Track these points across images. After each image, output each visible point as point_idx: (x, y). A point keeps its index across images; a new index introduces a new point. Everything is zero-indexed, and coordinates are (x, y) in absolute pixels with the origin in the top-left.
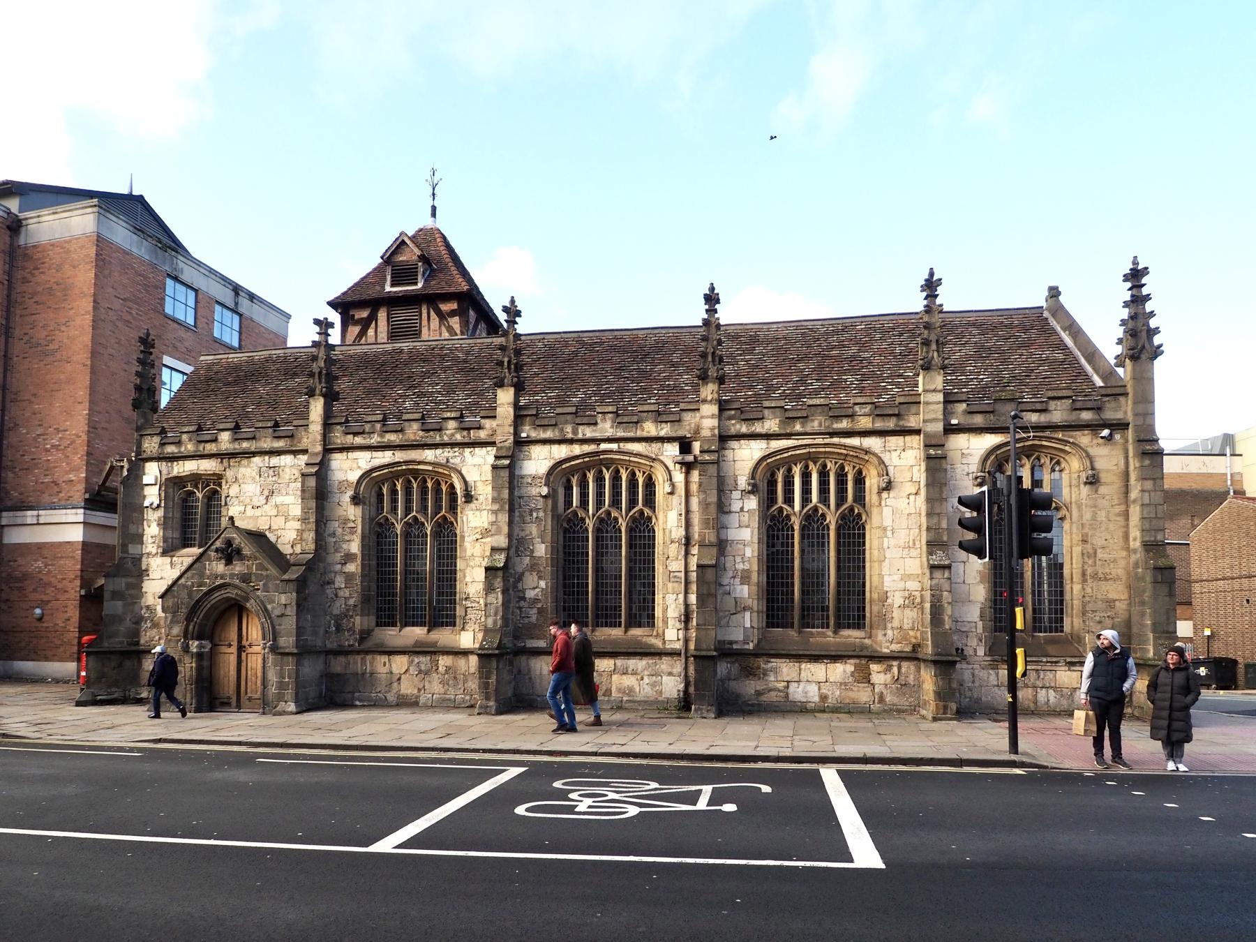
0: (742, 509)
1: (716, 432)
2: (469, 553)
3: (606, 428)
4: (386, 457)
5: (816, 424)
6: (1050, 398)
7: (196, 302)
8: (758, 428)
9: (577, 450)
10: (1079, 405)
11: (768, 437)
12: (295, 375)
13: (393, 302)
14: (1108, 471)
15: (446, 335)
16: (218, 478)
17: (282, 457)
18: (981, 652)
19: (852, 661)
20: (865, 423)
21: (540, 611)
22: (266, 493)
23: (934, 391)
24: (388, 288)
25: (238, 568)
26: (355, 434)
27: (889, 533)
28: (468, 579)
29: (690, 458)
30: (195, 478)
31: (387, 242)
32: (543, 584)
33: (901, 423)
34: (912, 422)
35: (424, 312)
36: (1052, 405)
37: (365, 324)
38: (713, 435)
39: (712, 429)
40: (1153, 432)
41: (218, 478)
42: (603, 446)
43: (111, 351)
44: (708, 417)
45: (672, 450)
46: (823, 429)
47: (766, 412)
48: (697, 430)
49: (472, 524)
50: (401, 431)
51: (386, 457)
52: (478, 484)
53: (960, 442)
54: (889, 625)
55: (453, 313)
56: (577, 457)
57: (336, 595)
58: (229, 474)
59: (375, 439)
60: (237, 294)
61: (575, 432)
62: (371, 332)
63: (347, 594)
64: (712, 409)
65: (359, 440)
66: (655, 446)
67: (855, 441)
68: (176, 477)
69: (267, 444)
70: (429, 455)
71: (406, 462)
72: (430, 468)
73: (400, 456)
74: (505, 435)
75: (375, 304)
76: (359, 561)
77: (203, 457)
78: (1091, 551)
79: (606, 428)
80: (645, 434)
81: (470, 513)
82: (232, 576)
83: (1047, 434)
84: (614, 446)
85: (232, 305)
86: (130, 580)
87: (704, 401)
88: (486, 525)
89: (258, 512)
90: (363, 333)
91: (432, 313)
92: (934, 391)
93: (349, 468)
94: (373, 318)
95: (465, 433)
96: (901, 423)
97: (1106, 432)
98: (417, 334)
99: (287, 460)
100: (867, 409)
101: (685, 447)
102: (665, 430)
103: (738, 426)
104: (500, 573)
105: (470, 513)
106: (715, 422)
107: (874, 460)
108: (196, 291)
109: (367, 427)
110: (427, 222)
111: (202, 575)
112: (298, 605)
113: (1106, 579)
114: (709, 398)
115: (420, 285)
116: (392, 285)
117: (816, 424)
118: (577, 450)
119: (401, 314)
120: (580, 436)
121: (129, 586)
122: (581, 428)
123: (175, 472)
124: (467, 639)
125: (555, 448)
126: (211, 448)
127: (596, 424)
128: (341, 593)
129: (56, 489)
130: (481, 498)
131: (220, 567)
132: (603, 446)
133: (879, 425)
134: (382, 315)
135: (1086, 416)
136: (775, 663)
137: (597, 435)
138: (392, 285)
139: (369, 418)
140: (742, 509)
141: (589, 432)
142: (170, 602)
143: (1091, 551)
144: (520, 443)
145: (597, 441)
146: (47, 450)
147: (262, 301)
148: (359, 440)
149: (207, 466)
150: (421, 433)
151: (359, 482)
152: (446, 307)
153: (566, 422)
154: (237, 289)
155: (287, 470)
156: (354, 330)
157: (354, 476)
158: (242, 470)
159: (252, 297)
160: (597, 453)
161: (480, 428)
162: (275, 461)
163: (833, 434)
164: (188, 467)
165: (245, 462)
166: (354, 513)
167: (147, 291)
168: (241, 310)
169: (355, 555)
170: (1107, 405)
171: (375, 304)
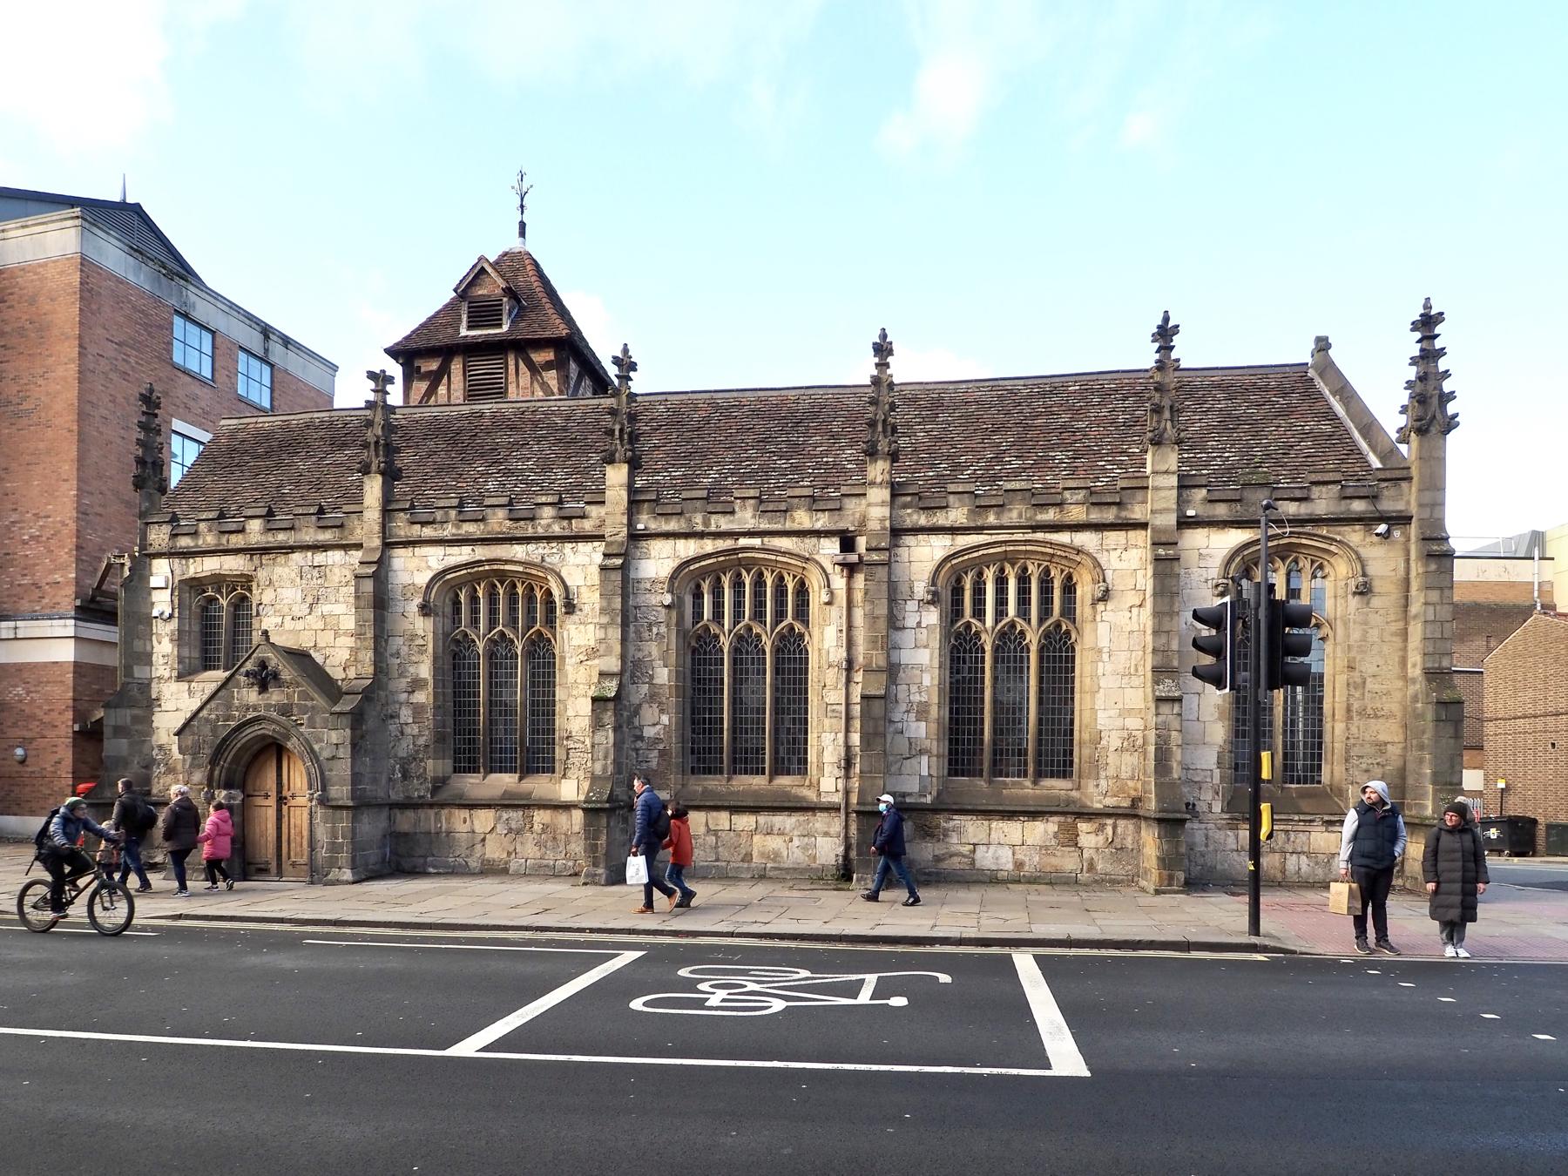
0: (919, 624)
1: (887, 524)
2: (571, 679)
3: (746, 518)
4: (463, 554)
5: (1014, 514)
6: (1313, 483)
7: (214, 347)
8: (941, 519)
9: (709, 546)
10: (1349, 492)
11: (953, 530)
12: (344, 445)
13: (472, 350)
14: (1382, 578)
15: (540, 394)
16: (247, 580)
17: (330, 553)
18: (1217, 807)
19: (1056, 819)
20: (1077, 514)
21: (663, 753)
22: (310, 600)
23: (1166, 472)
24: (464, 332)
25: (275, 696)
26: (424, 524)
27: (1105, 657)
28: (570, 713)
29: (853, 558)
30: (218, 580)
31: (460, 269)
32: (665, 719)
33: (1123, 514)
34: (1137, 513)
35: (511, 363)
36: (1316, 491)
37: (435, 379)
38: (884, 528)
39: (882, 520)
40: (1443, 528)
41: (247, 580)
42: (743, 542)
43: (105, 412)
44: (876, 505)
45: (831, 547)
46: (1023, 522)
47: (951, 498)
48: (863, 522)
49: (574, 642)
50: (483, 520)
51: (463, 554)
52: (583, 590)
53: (1196, 538)
54: (1103, 774)
55: (548, 366)
56: (709, 556)
57: (402, 733)
58: (262, 575)
59: (449, 531)
60: (267, 338)
61: (706, 523)
62: (442, 390)
63: (416, 731)
64: (880, 495)
65: (428, 532)
66: (810, 542)
67: (1063, 538)
69: (310, 535)
70: (519, 551)
71: (490, 561)
73: (482, 553)
74: (616, 528)
75: (447, 352)
76: (431, 689)
77: (227, 552)
78: (1359, 680)
79: (746, 518)
80: (796, 527)
81: (572, 628)
82: (268, 707)
83: (1308, 529)
84: (756, 542)
85: (261, 353)
86: (136, 712)
87: (872, 483)
88: (592, 643)
89: (300, 625)
91: (521, 365)
92: (1166, 472)
93: (416, 568)
94: (444, 370)
95: (565, 523)
96: (1123, 514)
97: (1382, 528)
99: (336, 556)
100: (1081, 495)
101: (848, 544)
102: (822, 521)
103: (915, 517)
104: (611, 705)
105: (572, 628)
106: (886, 511)
107: (1088, 562)
108: (213, 333)
109: (439, 515)
110: (515, 244)
111: (229, 706)
112: (354, 745)
113: (1376, 717)
114: (879, 480)
115: (505, 328)
116: (470, 328)
117: (1014, 514)
118: (709, 546)
119: (482, 366)
120: (713, 528)
121: (135, 719)
122: (714, 518)
123: (191, 573)
124: (570, 789)
125: (681, 543)
126: (236, 541)
127: (733, 513)
128: (408, 730)
129: (38, 593)
130: (586, 608)
131: (252, 696)
132: (743, 542)
133: (1095, 516)
134: (456, 367)
135: (1358, 506)
136: (958, 820)
137: (735, 527)
138: (470, 328)
139: (441, 503)
140: (919, 624)
141: (724, 523)
142: (189, 740)
143: (1359, 680)
144: (635, 537)
145: (735, 535)
146: (25, 543)
147: (300, 347)
148: (428, 532)
149: (233, 565)
150: (508, 523)
151: (429, 586)
152: (539, 357)
153: (695, 511)
154: (266, 331)
155: (336, 570)
156: (421, 387)
157: (423, 579)
158: (278, 570)
159: (286, 341)
160: (735, 551)
161: (583, 517)
162: (320, 558)
163: (1036, 528)
164: (209, 565)
165: (281, 559)
166: (423, 627)
167: (149, 334)
168: (272, 359)
169: (425, 680)
170: (1386, 492)
171: (447, 352)
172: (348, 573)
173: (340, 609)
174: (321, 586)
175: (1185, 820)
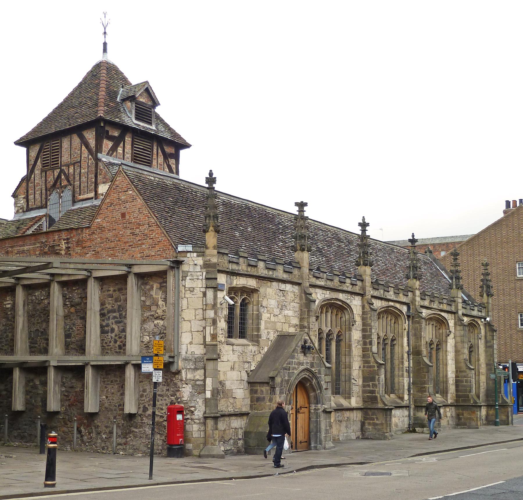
26: (317, 278)
28: (354, 368)
45: (404, 309)
50: (332, 280)
58: (262, 290)
68: (234, 287)
72: (341, 304)
73: (334, 295)
80: (399, 300)
90: (114, 149)
98: (149, 164)
99: (288, 287)
131: (301, 357)
132: (392, 304)
137: (389, 297)
155: (289, 294)
162: (283, 286)
165: (269, 283)
172: (293, 296)
173: (290, 313)
174: (284, 301)
175: (392, 409)
